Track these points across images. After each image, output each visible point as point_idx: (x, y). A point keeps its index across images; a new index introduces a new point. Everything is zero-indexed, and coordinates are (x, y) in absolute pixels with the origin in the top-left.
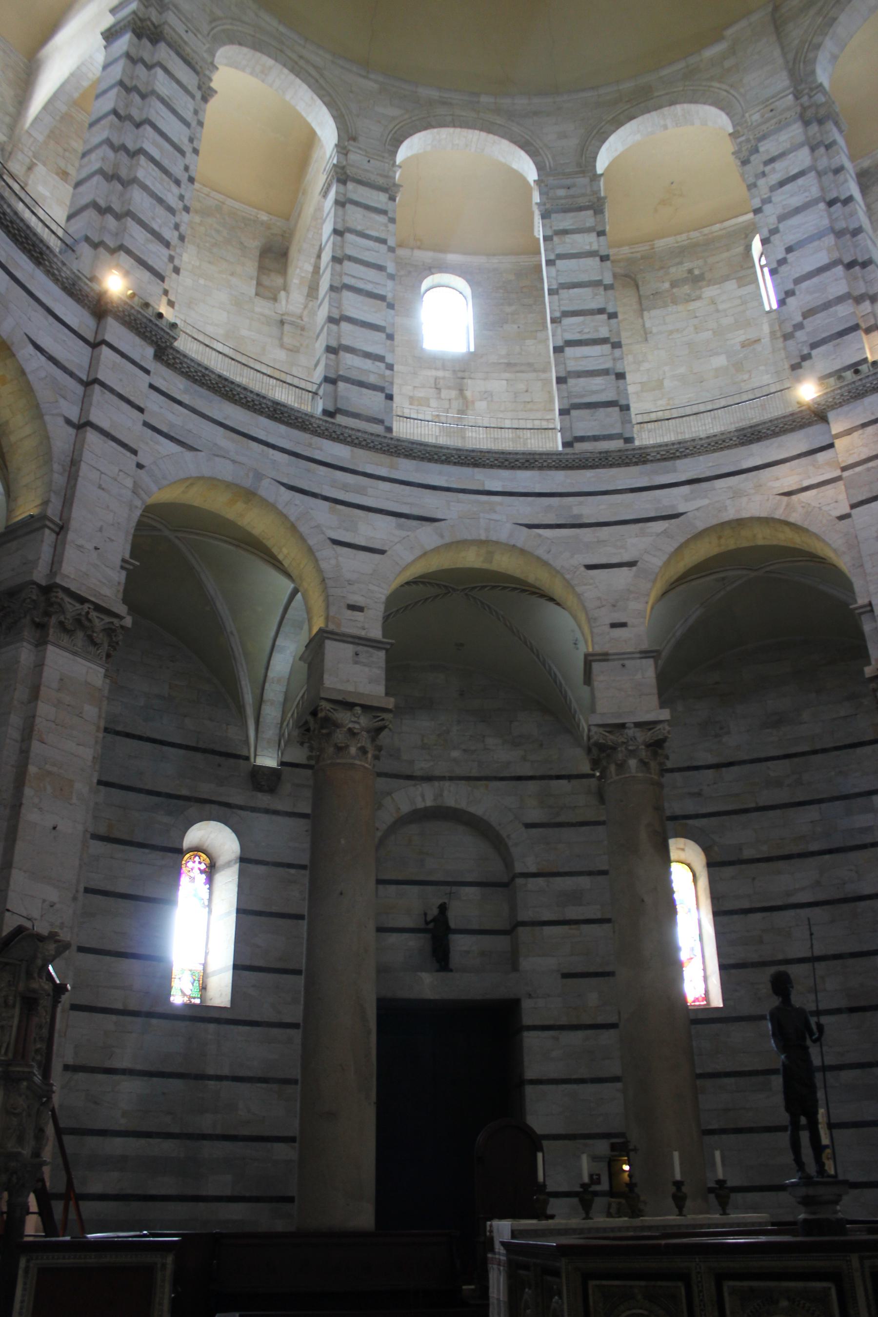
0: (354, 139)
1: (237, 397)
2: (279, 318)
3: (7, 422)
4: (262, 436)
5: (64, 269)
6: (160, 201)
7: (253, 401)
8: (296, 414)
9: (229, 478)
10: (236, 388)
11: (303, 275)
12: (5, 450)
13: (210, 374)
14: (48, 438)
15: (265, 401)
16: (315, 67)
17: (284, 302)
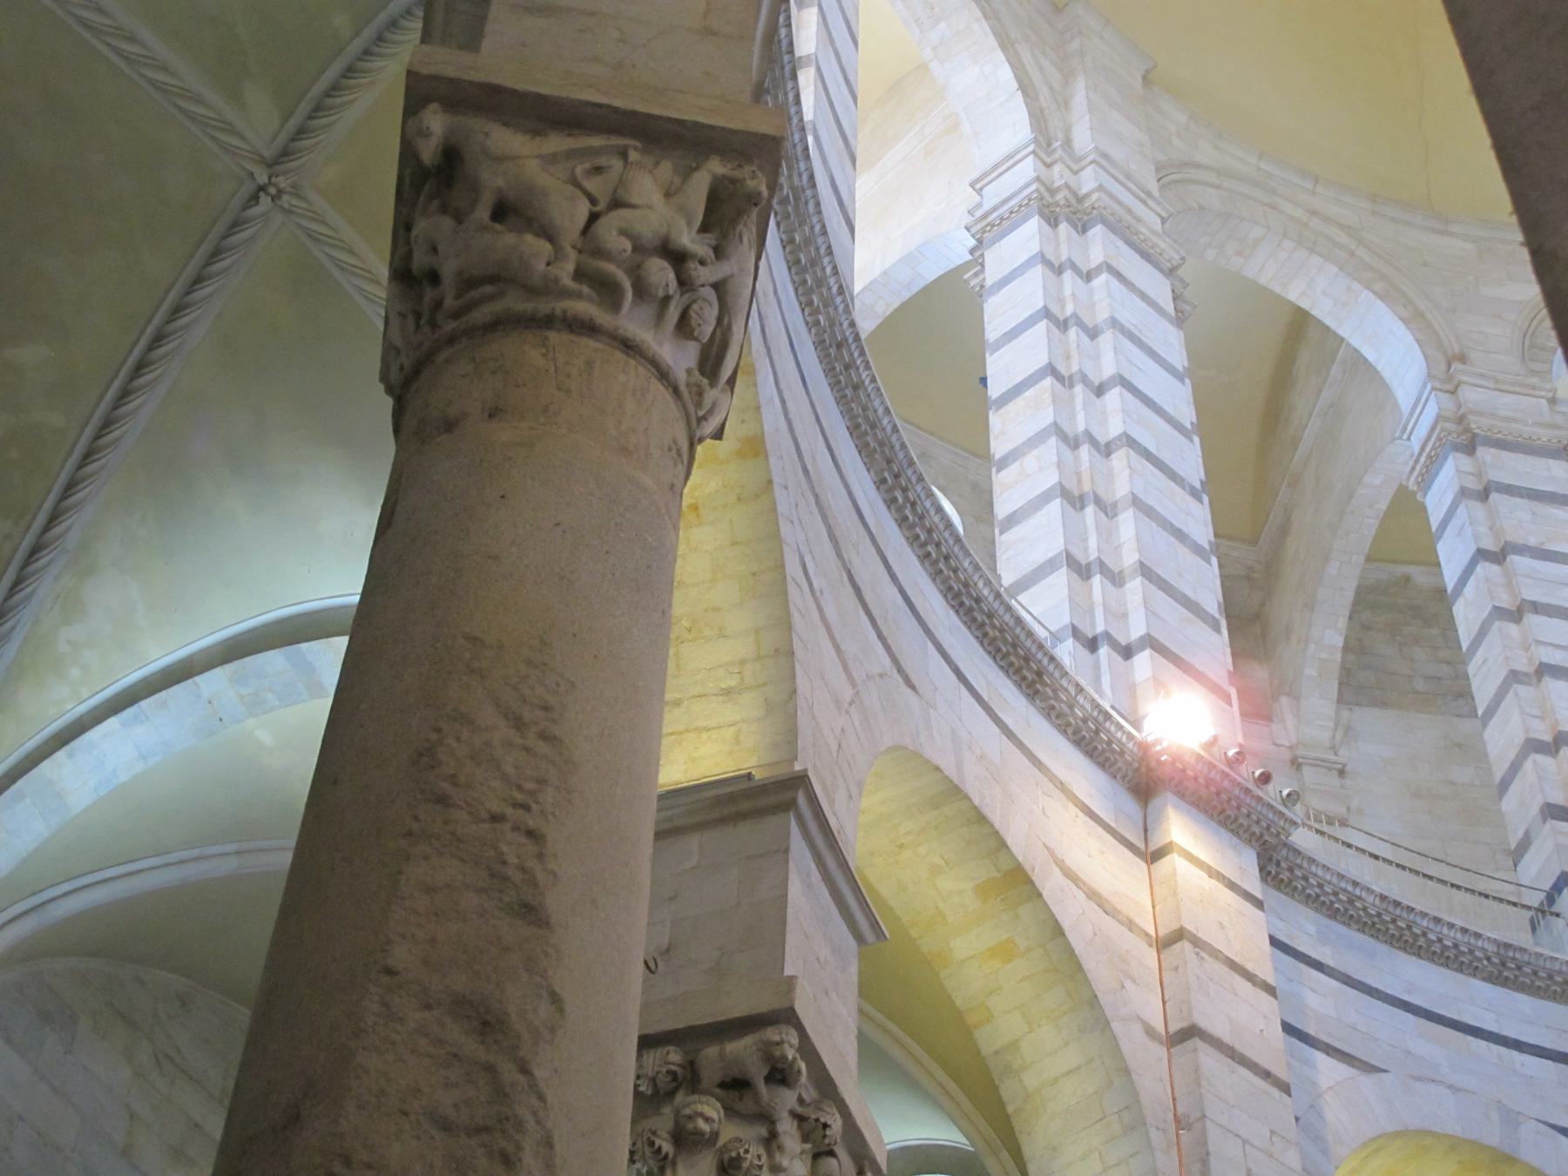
0: (1462, 359)
1: (1421, 942)
2: (1288, 755)
3: (1014, 1045)
4: (1489, 1025)
5: (1080, 699)
6: (1180, 535)
7: (1456, 946)
8: (1548, 965)
9: (1455, 1129)
10: (1418, 920)
11: (1324, 656)
12: (1010, 1109)
13: (1364, 895)
14: (1126, 1072)
15: (1480, 943)
16: (1346, 228)
17: (1290, 720)
